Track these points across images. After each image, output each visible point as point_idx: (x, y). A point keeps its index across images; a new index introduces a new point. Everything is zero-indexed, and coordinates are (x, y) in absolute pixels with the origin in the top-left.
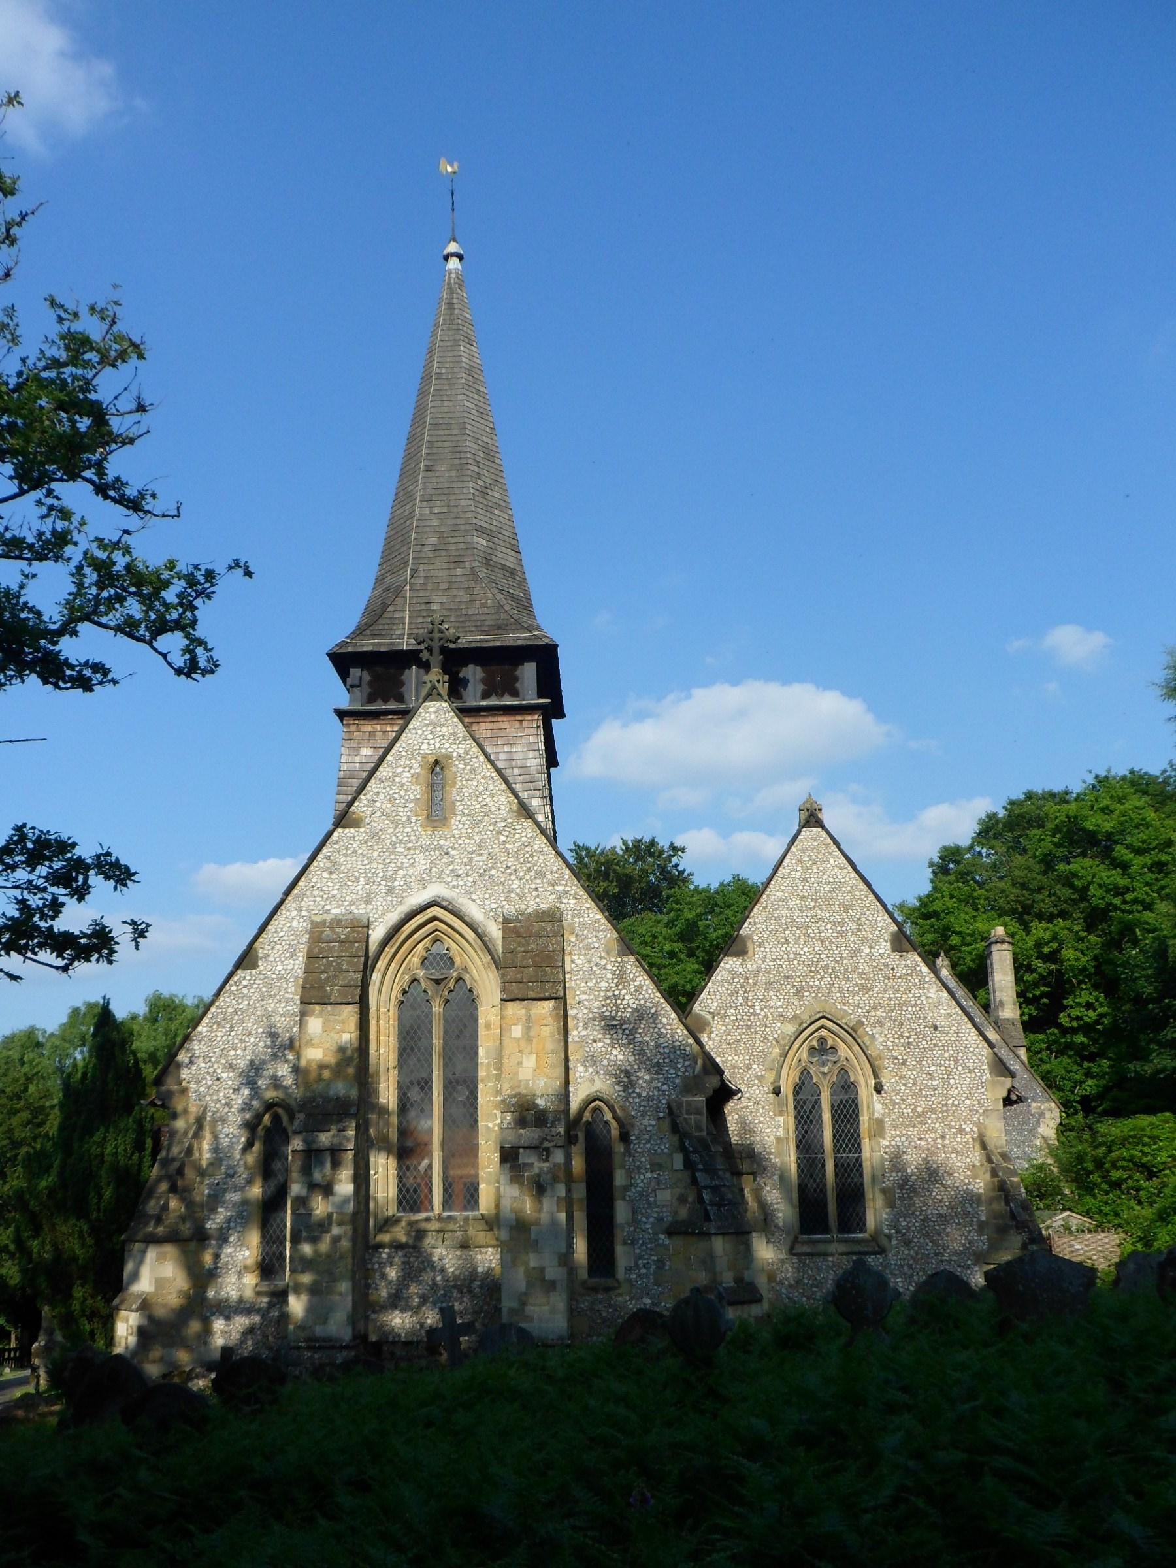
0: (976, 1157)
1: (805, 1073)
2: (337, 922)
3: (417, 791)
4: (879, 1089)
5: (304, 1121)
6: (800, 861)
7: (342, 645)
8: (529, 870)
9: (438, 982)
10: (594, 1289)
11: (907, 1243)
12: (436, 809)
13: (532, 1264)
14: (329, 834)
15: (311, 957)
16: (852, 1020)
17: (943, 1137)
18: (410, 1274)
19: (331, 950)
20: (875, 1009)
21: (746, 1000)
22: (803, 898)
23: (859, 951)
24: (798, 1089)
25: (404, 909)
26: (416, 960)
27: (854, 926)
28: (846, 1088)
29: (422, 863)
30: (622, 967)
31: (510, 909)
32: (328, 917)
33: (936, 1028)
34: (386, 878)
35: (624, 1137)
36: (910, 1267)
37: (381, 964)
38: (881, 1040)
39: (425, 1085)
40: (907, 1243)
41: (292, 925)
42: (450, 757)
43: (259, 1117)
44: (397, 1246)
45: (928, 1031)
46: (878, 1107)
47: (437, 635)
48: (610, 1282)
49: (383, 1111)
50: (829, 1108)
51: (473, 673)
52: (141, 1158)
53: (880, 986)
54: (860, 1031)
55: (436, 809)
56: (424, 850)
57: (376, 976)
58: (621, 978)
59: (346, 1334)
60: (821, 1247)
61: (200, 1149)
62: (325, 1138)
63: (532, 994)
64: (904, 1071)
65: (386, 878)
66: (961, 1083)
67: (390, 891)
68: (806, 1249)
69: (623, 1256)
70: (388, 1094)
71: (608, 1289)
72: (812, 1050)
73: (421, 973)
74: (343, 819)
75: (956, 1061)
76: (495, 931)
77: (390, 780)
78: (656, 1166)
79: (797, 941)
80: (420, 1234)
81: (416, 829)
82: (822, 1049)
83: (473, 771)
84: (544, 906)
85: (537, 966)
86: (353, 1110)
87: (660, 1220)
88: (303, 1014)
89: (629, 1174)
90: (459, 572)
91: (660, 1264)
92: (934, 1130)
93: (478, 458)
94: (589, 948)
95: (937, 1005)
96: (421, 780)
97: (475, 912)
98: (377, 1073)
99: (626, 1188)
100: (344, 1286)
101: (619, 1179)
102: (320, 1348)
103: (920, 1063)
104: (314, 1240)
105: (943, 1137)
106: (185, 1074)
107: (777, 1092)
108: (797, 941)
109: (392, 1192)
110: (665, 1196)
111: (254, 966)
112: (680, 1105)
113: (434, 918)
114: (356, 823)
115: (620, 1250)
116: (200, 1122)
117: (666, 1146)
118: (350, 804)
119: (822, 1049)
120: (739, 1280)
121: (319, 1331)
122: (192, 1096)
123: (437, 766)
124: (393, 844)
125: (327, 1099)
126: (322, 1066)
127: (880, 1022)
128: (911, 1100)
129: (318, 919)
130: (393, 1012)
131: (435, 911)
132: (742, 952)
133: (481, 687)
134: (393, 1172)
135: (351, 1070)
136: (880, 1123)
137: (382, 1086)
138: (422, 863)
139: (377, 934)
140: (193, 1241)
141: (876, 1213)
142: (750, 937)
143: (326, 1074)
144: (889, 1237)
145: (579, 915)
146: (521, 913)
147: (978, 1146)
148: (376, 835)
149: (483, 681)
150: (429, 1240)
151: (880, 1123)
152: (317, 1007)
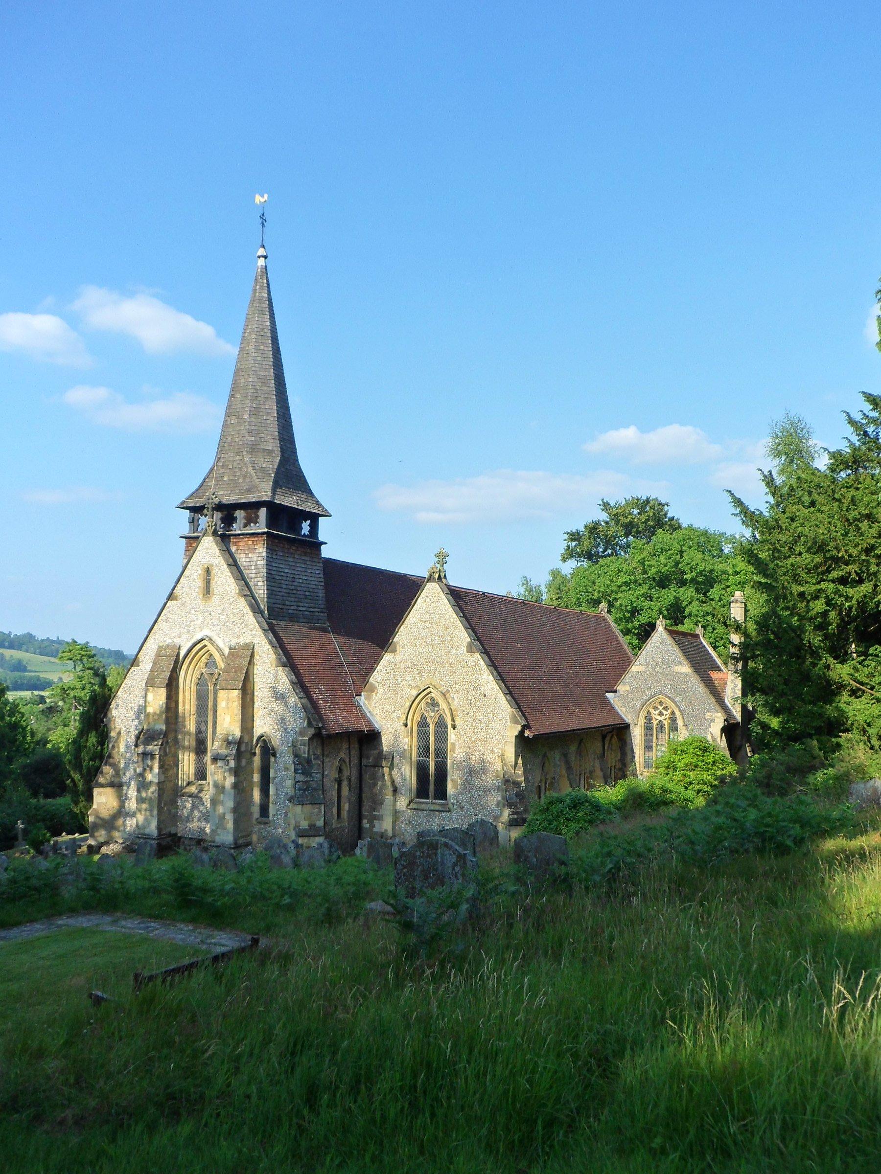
0: (498, 766)
3: (200, 583)
4: (454, 727)
5: (164, 736)
7: (184, 502)
9: (212, 674)
10: (260, 823)
11: (462, 808)
12: (207, 590)
14: (166, 604)
15: (155, 664)
16: (444, 689)
18: (194, 807)
19: (162, 660)
20: (456, 684)
25: (194, 640)
26: (202, 664)
28: (441, 724)
29: (201, 618)
30: (277, 671)
31: (234, 643)
32: (165, 644)
35: (274, 755)
37: (185, 667)
38: (457, 701)
39: (206, 723)
40: (462, 808)
41: (151, 648)
43: (140, 733)
44: (191, 796)
45: (481, 697)
47: (210, 501)
49: (189, 733)
50: (432, 734)
51: (240, 514)
52: (102, 749)
55: (207, 590)
57: (182, 673)
58: (276, 677)
60: (423, 806)
61: (118, 748)
62: (150, 748)
63: (229, 687)
64: (467, 718)
67: (189, 631)
70: (191, 726)
71: (265, 823)
73: (204, 671)
74: (171, 597)
76: (226, 651)
78: (287, 769)
80: (201, 791)
81: (199, 601)
84: (248, 641)
85: (236, 672)
87: (287, 794)
88: (146, 691)
89: (275, 771)
90: (238, 458)
93: (257, 387)
96: (202, 577)
97: (221, 644)
98: (184, 717)
99: (274, 778)
100: (155, 812)
101: (272, 775)
104: (147, 792)
106: (114, 712)
107: (406, 725)
109: (192, 771)
110: (289, 783)
111: (138, 666)
112: (297, 741)
113: (205, 646)
114: (176, 599)
116: (119, 733)
117: (289, 760)
118: (175, 587)
119: (434, 704)
120: (312, 826)
121: (147, 831)
122: (117, 724)
123: (208, 571)
125: (154, 731)
126: (155, 713)
127: (457, 692)
128: (469, 734)
130: (194, 688)
132: (394, 651)
133: (244, 521)
134: (192, 762)
135: (164, 716)
136: (453, 744)
137: (187, 723)
138: (201, 618)
140: (117, 786)
141: (451, 789)
143: (156, 717)
144: (453, 804)
146: (238, 644)
149: (245, 518)
150: (201, 795)
151: (453, 744)
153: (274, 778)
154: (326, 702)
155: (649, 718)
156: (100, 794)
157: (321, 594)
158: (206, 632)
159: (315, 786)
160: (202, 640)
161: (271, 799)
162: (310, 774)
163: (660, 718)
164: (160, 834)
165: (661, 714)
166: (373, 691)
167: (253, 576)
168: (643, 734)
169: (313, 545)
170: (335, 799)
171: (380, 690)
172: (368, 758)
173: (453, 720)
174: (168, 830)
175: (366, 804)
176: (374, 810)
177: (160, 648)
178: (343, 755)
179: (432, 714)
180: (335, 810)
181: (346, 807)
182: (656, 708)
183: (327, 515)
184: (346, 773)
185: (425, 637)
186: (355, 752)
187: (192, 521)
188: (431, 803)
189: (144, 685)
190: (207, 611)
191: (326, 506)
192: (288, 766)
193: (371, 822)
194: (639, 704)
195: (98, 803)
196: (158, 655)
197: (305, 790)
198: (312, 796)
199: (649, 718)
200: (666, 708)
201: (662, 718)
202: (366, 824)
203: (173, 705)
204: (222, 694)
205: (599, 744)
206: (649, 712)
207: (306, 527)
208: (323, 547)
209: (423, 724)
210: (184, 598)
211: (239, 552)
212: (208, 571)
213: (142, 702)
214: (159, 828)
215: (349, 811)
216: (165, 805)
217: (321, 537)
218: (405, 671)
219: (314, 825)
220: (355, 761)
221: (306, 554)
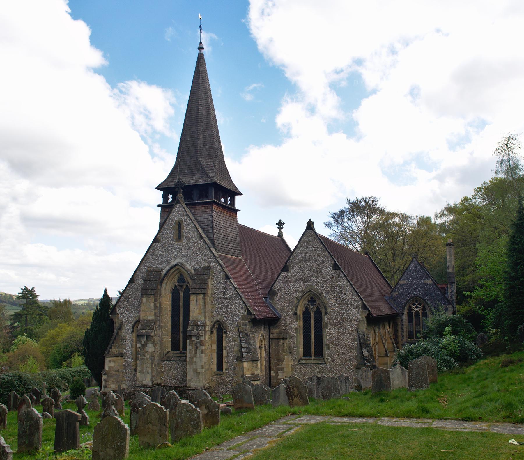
1: (306, 308)
2: (154, 269)
4: (326, 313)
6: (306, 241)
8: (202, 254)
10: (217, 374)
13: (195, 368)
15: (145, 281)
17: (346, 329)
21: (288, 285)
22: (306, 253)
23: (323, 269)
24: (304, 313)
25: (170, 266)
27: (322, 262)
32: (151, 269)
33: (345, 294)
34: (166, 257)
35: (226, 333)
36: (333, 368)
38: (328, 298)
40: (333, 361)
42: (182, 221)
46: (326, 319)
48: (221, 372)
54: (322, 295)
55: (179, 237)
56: (175, 249)
59: (150, 384)
60: (308, 361)
63: (197, 292)
64: (335, 308)
65: (166, 257)
66: (352, 312)
67: (167, 261)
68: (303, 362)
69: (225, 366)
71: (220, 375)
72: (309, 301)
73: (176, 284)
75: (351, 305)
77: (167, 228)
78: (234, 341)
79: (304, 266)
82: (312, 301)
83: (188, 225)
86: (153, 324)
87: (234, 356)
89: (227, 342)
91: (234, 368)
92: (343, 327)
94: (218, 277)
95: (346, 287)
99: (226, 347)
101: (224, 344)
102: (144, 387)
103: (340, 305)
105: (346, 329)
107: (296, 314)
108: (304, 266)
109: (169, 345)
111: (134, 282)
115: (224, 364)
120: (253, 374)
123: (179, 224)
124: (168, 247)
127: (328, 292)
129: (149, 269)
131: (177, 267)
136: (327, 324)
138: (175, 253)
139: (164, 273)
142: (290, 266)
144: (328, 359)
145: (215, 267)
147: (356, 332)
148: (163, 244)
151: (327, 324)
152: (145, 296)
153: (226, 347)
154: (252, 300)
155: (410, 309)
156: (110, 361)
159: (253, 350)
160: (177, 265)
161: (224, 360)
163: (416, 309)
164: (153, 384)
165: (417, 307)
166: (275, 295)
167: (206, 227)
168: (407, 319)
171: (280, 294)
172: (273, 334)
173: (326, 309)
177: (148, 271)
178: (262, 332)
179: (312, 307)
182: (414, 304)
183: (240, 194)
186: (267, 331)
187: (165, 198)
188: (312, 359)
189: (138, 293)
190: (179, 248)
192: (236, 339)
194: (404, 302)
195: (109, 367)
197: (248, 353)
198: (253, 356)
199: (410, 309)
200: (420, 304)
201: (417, 310)
202: (273, 374)
203: (158, 305)
204: (192, 297)
205: (388, 325)
206: (410, 307)
208: (238, 212)
209: (306, 313)
211: (196, 213)
212: (179, 224)
213: (333, 262)
214: (152, 381)
216: (155, 366)
217: (237, 207)
218: (294, 282)
219: (254, 374)
220: (267, 336)
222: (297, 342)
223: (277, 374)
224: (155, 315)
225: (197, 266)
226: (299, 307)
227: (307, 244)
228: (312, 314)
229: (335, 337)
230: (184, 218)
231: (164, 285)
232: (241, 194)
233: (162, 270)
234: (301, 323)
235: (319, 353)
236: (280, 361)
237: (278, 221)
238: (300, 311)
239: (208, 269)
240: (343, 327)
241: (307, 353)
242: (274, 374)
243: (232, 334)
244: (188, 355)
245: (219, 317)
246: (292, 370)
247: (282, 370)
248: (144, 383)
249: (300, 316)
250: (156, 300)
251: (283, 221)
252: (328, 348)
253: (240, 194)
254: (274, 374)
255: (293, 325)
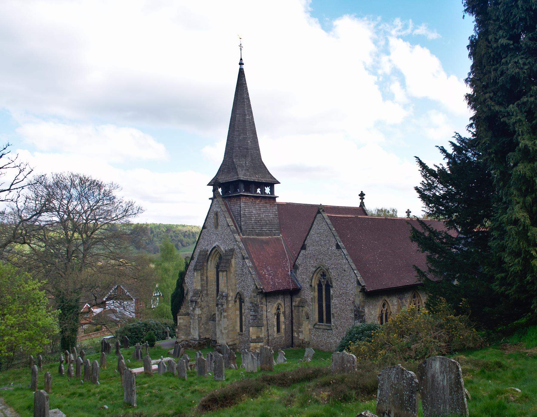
11: (337, 328)
23: (329, 248)
38: (333, 274)
41: (198, 250)
53: (333, 258)
60: (320, 327)
66: (350, 286)
82: (324, 275)
92: (343, 299)
95: (345, 264)
101: (243, 312)
107: (311, 286)
116: (188, 291)
120: (258, 337)
127: (333, 269)
136: (332, 296)
139: (209, 253)
148: (208, 230)
156: (180, 318)
157: (276, 221)
158: (217, 243)
162: (258, 312)
164: (200, 339)
169: (272, 198)
170: (276, 323)
171: (300, 269)
174: (204, 336)
175: (295, 324)
176: (299, 328)
177: (201, 251)
180: (275, 329)
181: (283, 327)
183: (278, 183)
184: (282, 310)
185: (318, 242)
188: (324, 325)
191: (278, 179)
193: (298, 334)
196: (199, 255)
198: (258, 323)
202: (295, 335)
203: (205, 278)
207: (267, 190)
208: (277, 199)
209: (320, 285)
210: (209, 228)
214: (200, 336)
215: (285, 329)
216: (202, 325)
217: (276, 194)
219: (259, 337)
220: (289, 304)
221: (266, 203)
222: (313, 309)
223: (299, 336)
224: (202, 286)
225: (227, 248)
226: (313, 280)
227: (318, 226)
228: (324, 287)
229: (338, 307)
230: (219, 210)
231: (209, 262)
232: (279, 183)
233: (208, 251)
234: (316, 294)
235: (329, 321)
236: (300, 325)
237: (360, 193)
238: (315, 283)
239: (232, 250)
240: (343, 299)
241: (321, 320)
242: (297, 336)
243: (247, 304)
244: (217, 319)
245: (240, 289)
246: (310, 333)
247: (302, 332)
248: (195, 337)
249: (314, 288)
250: (202, 275)
251: (364, 192)
252: (334, 317)
253: (278, 183)
254: (297, 336)
255: (309, 295)
